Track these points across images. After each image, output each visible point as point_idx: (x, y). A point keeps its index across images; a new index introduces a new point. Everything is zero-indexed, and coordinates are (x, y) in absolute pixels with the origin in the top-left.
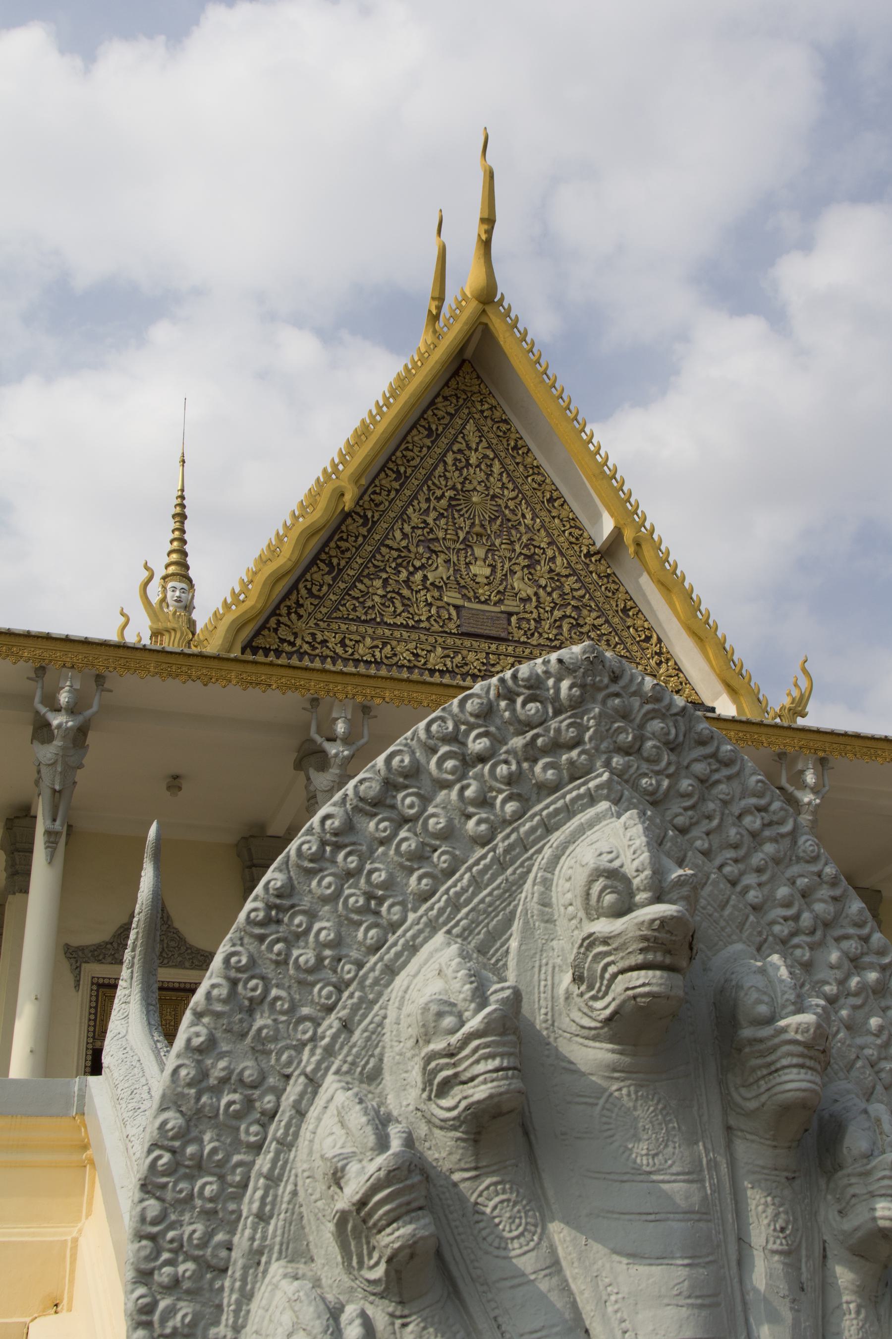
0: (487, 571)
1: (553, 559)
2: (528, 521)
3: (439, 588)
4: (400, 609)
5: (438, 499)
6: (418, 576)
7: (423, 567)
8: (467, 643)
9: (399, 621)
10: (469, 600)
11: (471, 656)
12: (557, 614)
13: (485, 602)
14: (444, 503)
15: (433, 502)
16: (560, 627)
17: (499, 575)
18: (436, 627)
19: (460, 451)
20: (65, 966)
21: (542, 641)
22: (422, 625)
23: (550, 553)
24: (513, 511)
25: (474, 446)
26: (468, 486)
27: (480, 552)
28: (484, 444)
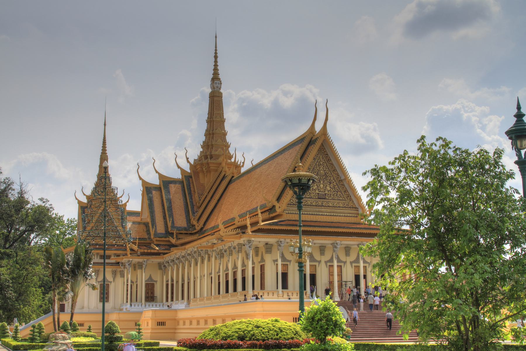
0: (323, 186)
1: (334, 182)
2: (330, 175)
3: (315, 190)
4: (309, 194)
5: (315, 172)
7: (313, 186)
8: (319, 200)
9: (309, 197)
11: (320, 202)
12: (334, 193)
14: (316, 173)
15: (314, 173)
16: (334, 196)
17: (325, 186)
18: (314, 198)
19: (319, 162)
21: (331, 198)
22: (313, 197)
23: (333, 181)
24: (327, 173)
25: (321, 160)
26: (320, 169)
27: (322, 182)
28: (323, 160)
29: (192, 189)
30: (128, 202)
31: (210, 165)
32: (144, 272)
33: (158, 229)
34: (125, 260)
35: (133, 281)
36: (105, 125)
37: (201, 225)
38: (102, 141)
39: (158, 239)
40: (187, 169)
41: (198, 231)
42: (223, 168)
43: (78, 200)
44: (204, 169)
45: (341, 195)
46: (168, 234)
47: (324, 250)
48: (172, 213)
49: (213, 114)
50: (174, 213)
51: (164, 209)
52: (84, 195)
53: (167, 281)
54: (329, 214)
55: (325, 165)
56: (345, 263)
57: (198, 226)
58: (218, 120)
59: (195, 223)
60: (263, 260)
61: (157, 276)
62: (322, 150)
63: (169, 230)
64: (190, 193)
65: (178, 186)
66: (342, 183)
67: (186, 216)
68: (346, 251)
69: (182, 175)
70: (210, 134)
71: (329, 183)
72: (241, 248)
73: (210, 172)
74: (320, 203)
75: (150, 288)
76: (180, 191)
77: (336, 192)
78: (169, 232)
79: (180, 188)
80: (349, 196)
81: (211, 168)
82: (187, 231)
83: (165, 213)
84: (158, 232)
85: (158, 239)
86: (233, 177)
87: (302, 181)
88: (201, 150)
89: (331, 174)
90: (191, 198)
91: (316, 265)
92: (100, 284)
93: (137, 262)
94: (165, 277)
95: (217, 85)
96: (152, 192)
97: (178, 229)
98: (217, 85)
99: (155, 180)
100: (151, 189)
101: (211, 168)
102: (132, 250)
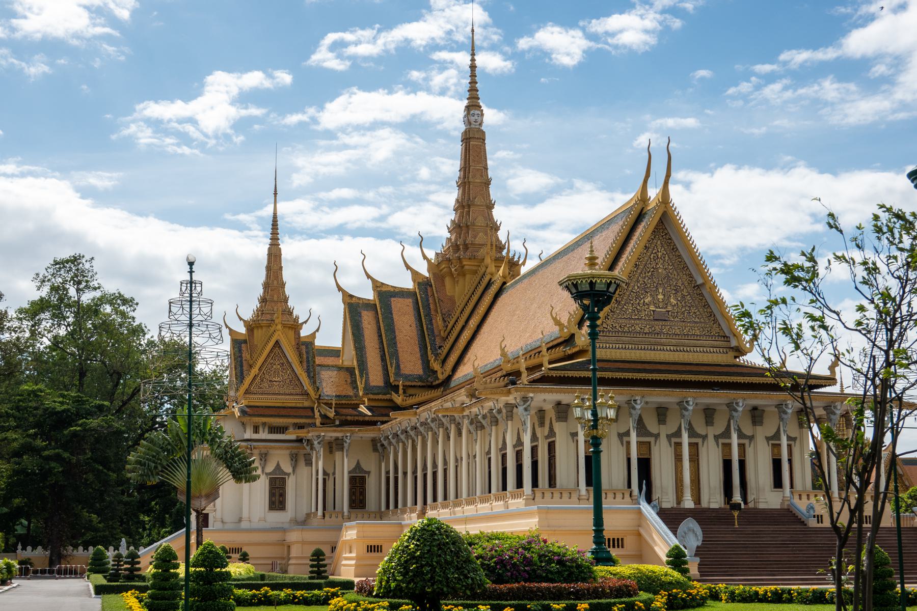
0: (662, 297)
6: (642, 301)
8: (656, 322)
10: (657, 308)
12: (684, 309)
13: (662, 308)
20: (570, 437)
27: (661, 291)
29: (432, 306)
30: (318, 330)
31: (465, 263)
32: (347, 456)
33: (371, 378)
34: (311, 434)
35: (328, 471)
36: (275, 194)
38: (271, 223)
39: (372, 396)
40: (423, 269)
41: (443, 382)
44: (453, 270)
45: (698, 313)
47: (665, 415)
49: (469, 170)
50: (400, 350)
51: (382, 342)
52: (241, 319)
53: (388, 472)
54: (675, 348)
55: (667, 258)
56: (705, 437)
57: (442, 373)
59: (436, 366)
60: (552, 433)
61: (369, 463)
62: (661, 231)
63: (391, 381)
64: (428, 315)
65: (409, 301)
66: (698, 291)
67: (422, 356)
68: (706, 417)
69: (414, 281)
70: (463, 207)
71: (674, 292)
72: (512, 411)
73: (464, 275)
74: (658, 329)
75: (358, 484)
77: (687, 308)
78: (390, 383)
79: (411, 305)
80: (712, 314)
81: (466, 267)
82: (423, 382)
83: (384, 351)
84: (372, 384)
85: (372, 396)
87: (597, 285)
88: (449, 235)
89: (678, 274)
90: (430, 322)
91: (649, 443)
92: (270, 478)
93: (333, 439)
94: (383, 465)
95: (476, 117)
96: (360, 313)
97: (407, 377)
98: (476, 117)
101: (466, 267)
102: (324, 417)
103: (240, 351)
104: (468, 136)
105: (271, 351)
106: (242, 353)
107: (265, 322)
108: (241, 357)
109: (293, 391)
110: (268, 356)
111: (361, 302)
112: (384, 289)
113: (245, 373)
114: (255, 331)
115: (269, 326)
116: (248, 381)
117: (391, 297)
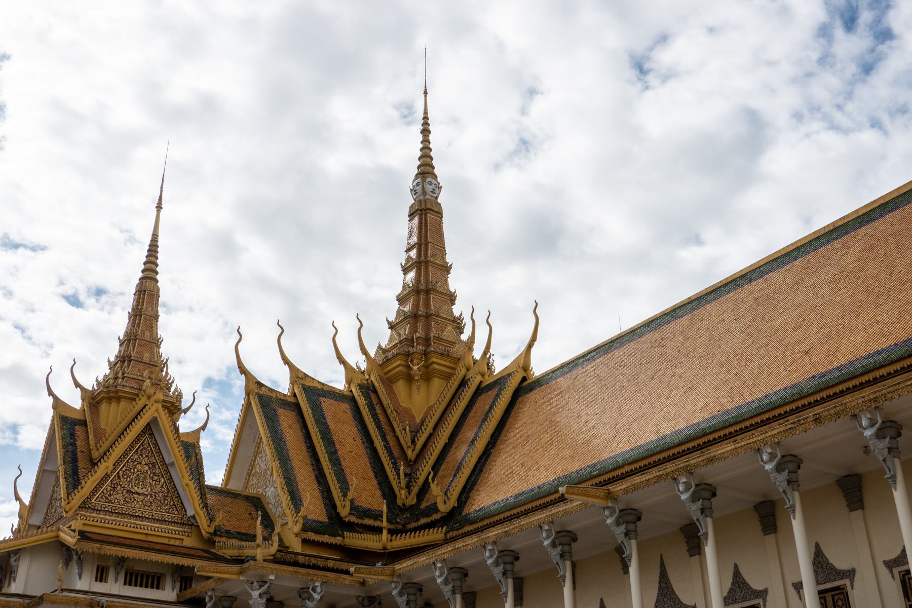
30: (203, 427)
36: (159, 207)
37: (453, 502)
42: (468, 370)
43: (56, 399)
46: (336, 524)
48: (343, 470)
52: (77, 385)
58: (437, 262)
65: (345, 407)
76: (349, 416)
86: (524, 379)
96: (275, 410)
99: (281, 383)
100: (272, 401)
101: (435, 366)
103: (72, 435)
104: (423, 207)
105: (137, 439)
106: (75, 440)
107: (128, 390)
108: (74, 444)
109: (167, 517)
110: (131, 446)
111: (274, 395)
112: (308, 383)
113: (81, 472)
114: (104, 407)
115: (133, 399)
116: (89, 484)
117: (319, 395)
